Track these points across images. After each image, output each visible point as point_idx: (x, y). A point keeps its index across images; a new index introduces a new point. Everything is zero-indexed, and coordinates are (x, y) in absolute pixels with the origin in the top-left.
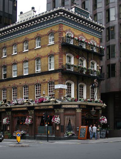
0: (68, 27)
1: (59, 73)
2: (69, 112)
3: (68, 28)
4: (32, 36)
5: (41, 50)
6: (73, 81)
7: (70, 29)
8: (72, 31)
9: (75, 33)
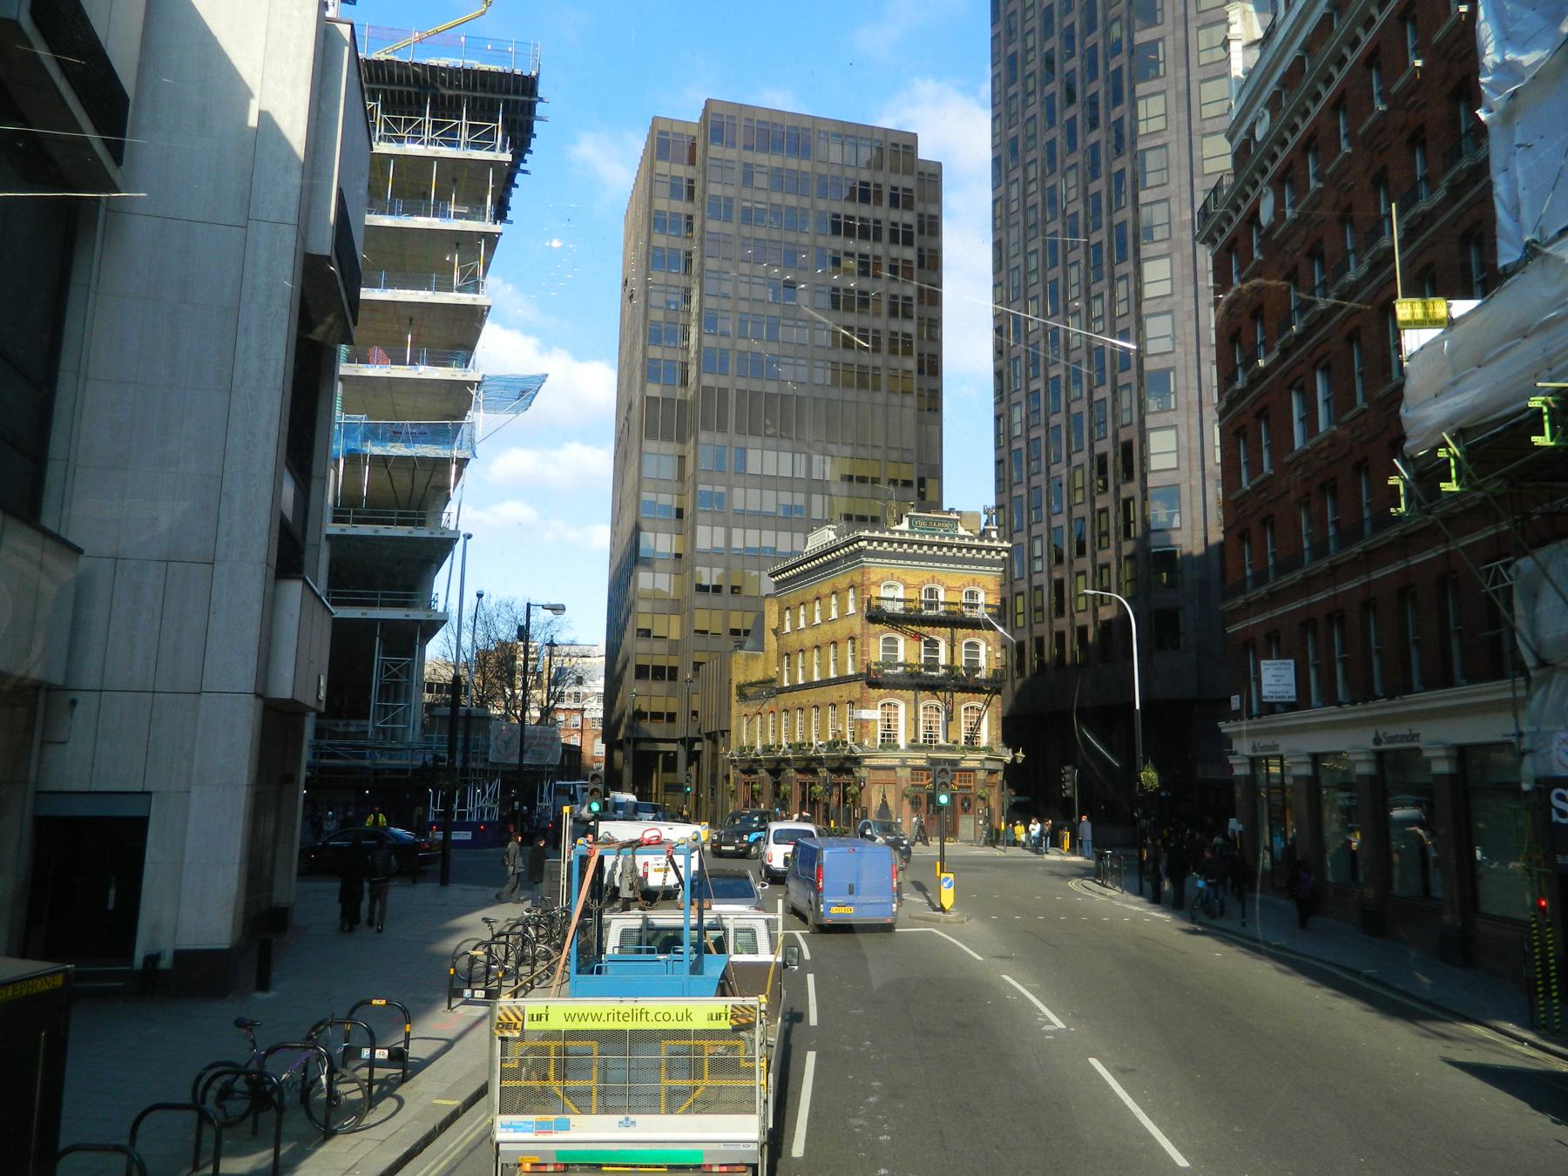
2: (882, 775)
3: (886, 571)
4: (825, 589)
5: (838, 625)
6: (901, 698)
7: (892, 574)
9: (911, 580)
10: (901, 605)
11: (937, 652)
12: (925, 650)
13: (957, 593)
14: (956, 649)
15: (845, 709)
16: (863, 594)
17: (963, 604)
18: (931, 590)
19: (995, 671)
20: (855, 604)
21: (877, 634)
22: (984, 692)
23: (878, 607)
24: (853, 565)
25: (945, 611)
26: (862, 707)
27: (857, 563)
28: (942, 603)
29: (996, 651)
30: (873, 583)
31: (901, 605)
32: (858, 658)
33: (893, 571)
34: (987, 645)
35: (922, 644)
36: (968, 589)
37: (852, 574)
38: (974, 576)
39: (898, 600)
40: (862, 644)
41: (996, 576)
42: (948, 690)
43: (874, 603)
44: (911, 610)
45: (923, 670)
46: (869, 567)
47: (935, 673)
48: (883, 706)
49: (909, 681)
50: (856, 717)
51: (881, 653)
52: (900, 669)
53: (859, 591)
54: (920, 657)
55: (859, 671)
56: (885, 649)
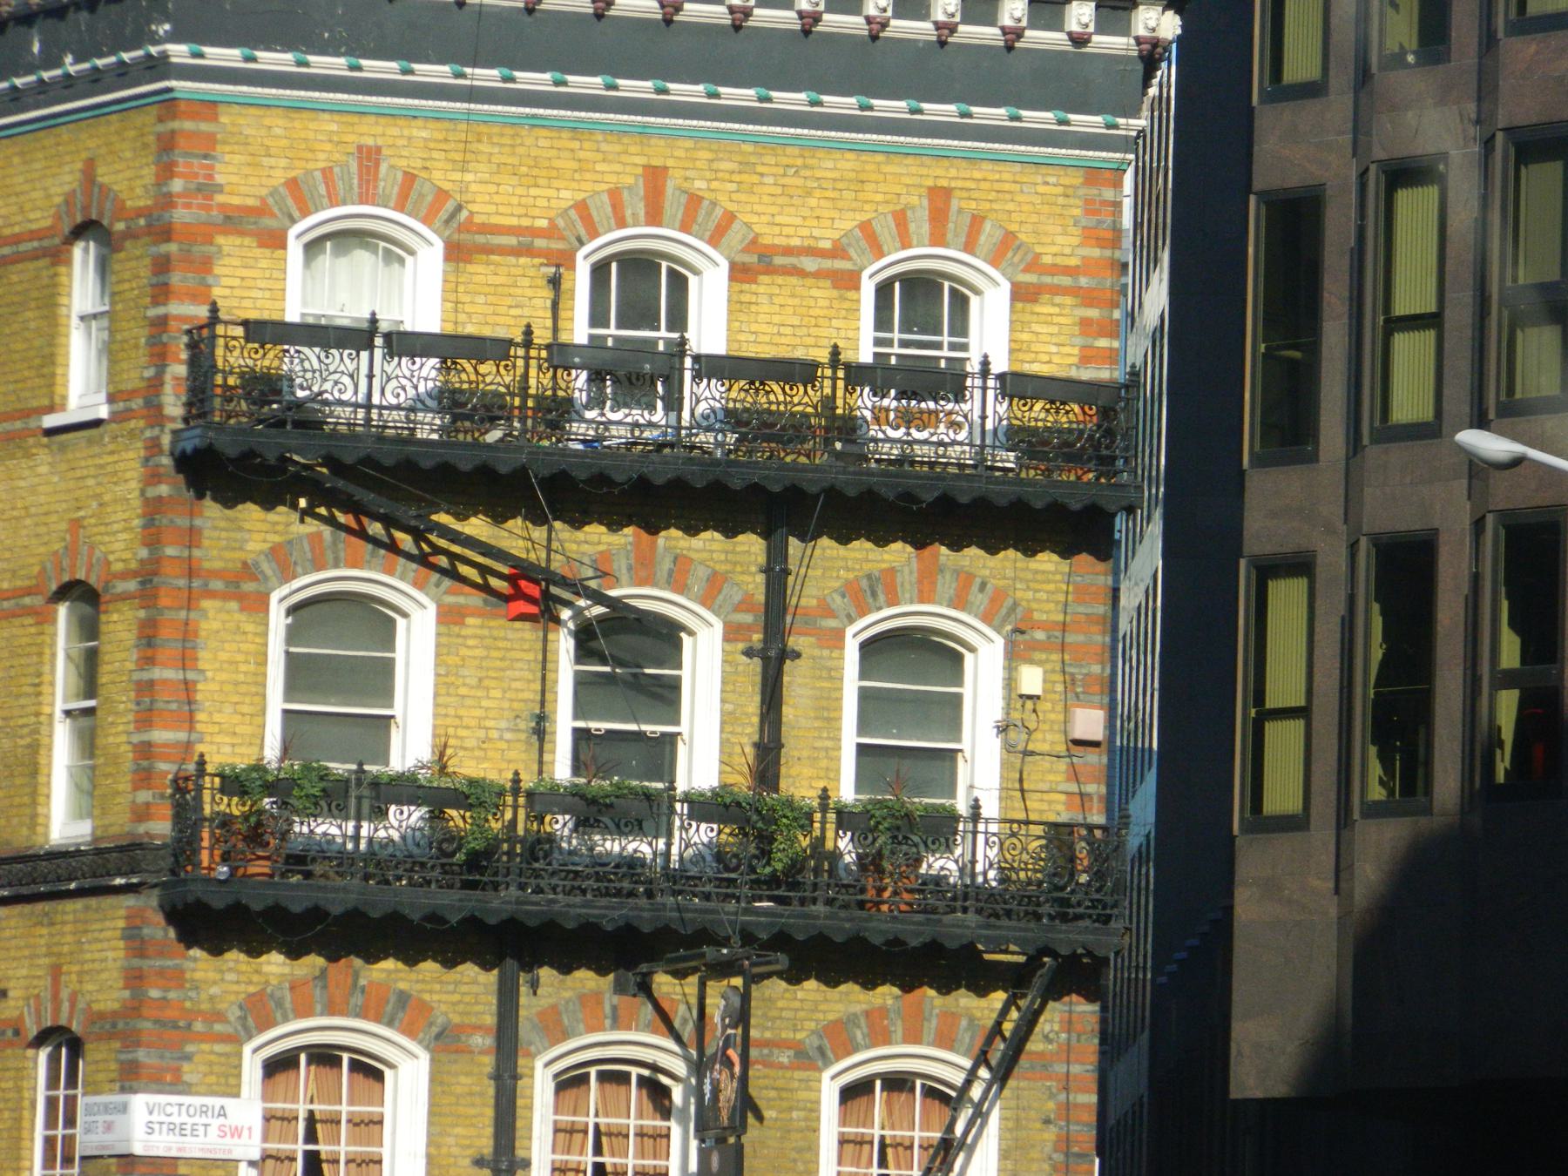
0: (330, 125)
1: (129, 901)
7: (369, 158)
8: (410, 178)
10: (426, 373)
11: (666, 696)
12: (583, 684)
13: (822, 293)
14: (796, 678)
15: (23, 1075)
16: (162, 292)
17: (857, 375)
18: (639, 266)
19: (1059, 834)
20: (112, 352)
21: (248, 571)
22: (980, 978)
23: (265, 387)
24: (95, 81)
25: (733, 418)
26: (130, 1078)
27: (123, 75)
28: (710, 367)
29: (1072, 690)
30: (234, 221)
31: (426, 373)
32: (119, 735)
33: (369, 133)
34: (1014, 656)
35: (564, 644)
36: (897, 260)
37: (90, 140)
38: (943, 175)
39: (404, 344)
40: (148, 637)
41: (1093, 174)
42: (723, 969)
43: (234, 357)
44: (492, 410)
45: (560, 824)
46: (210, 107)
47: (641, 847)
48: (277, 1066)
49: (453, 902)
50: (86, 1142)
51: (276, 702)
52: (404, 820)
53: (135, 263)
54: (541, 729)
55: (120, 824)
56: (300, 674)
